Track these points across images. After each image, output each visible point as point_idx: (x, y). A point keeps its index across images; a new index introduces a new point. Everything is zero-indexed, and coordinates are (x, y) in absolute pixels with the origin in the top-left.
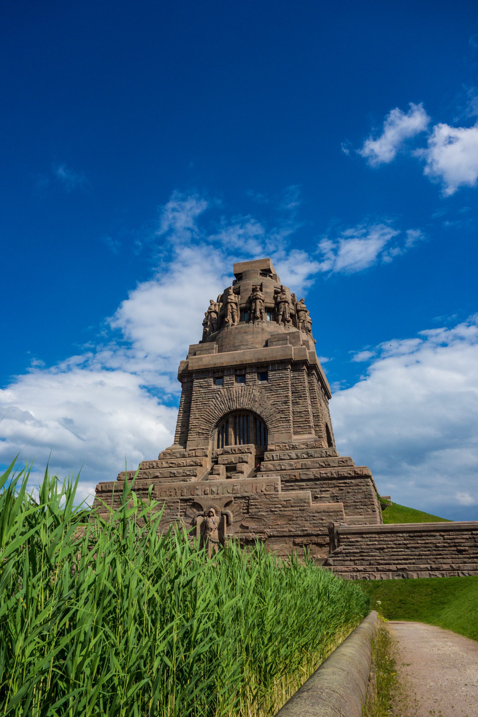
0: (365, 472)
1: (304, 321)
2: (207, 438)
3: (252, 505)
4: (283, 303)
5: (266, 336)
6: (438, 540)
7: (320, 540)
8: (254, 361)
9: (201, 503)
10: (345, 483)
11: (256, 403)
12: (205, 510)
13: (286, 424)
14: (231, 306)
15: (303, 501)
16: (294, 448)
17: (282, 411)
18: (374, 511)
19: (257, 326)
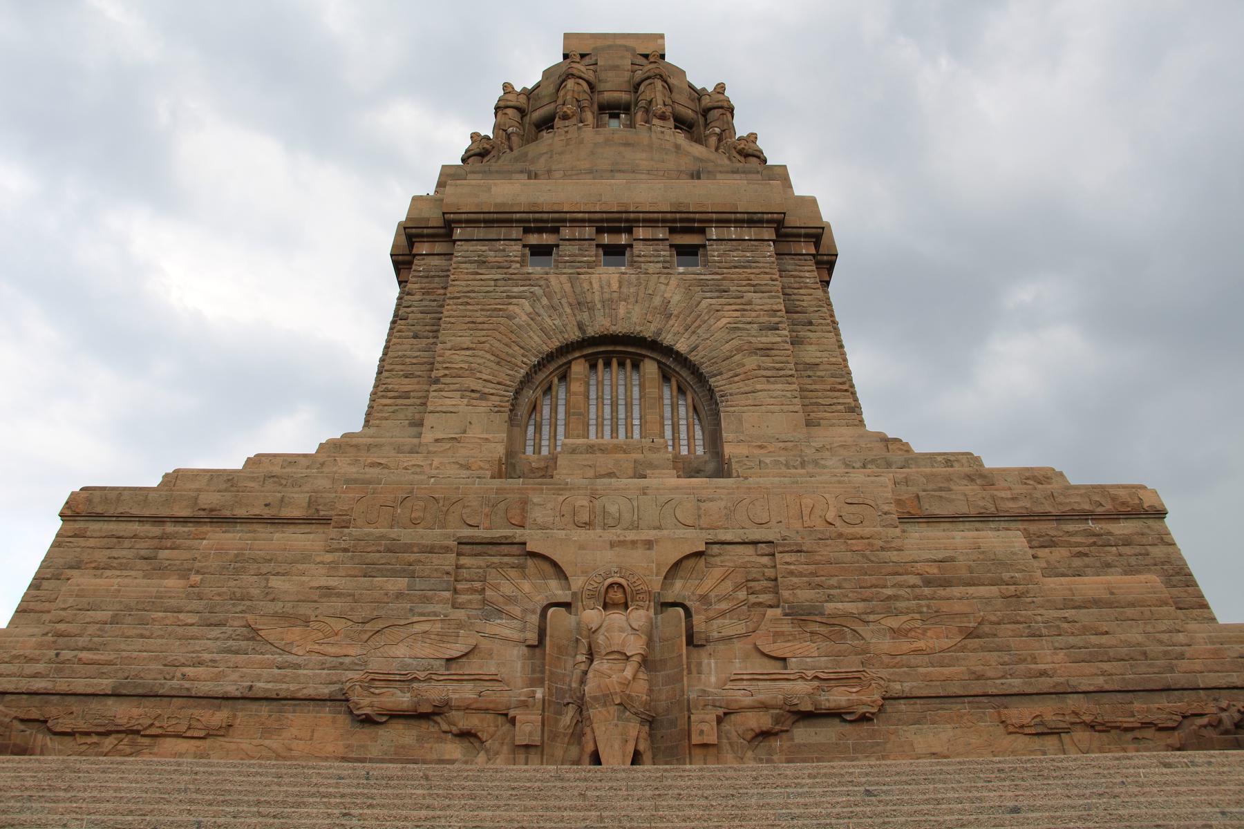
11: (671, 322)
12: (577, 583)
13: (779, 386)
17: (766, 350)
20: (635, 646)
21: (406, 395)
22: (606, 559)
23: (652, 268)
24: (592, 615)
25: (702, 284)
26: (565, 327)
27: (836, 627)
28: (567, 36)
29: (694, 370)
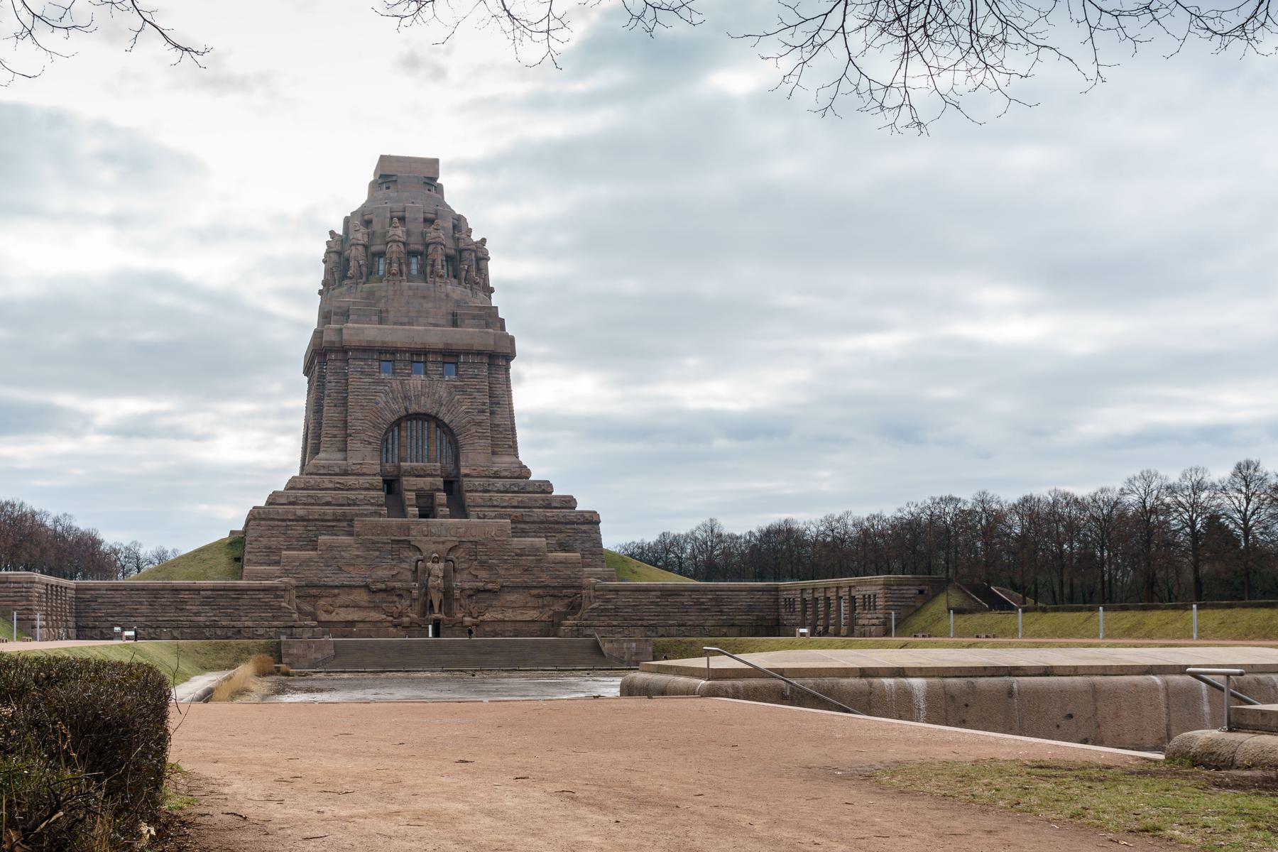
5: (450, 307)
6: (686, 600)
7: (555, 592)
8: (441, 346)
9: (420, 546)
15: (535, 550)
16: (497, 476)
17: (479, 424)
20: (441, 575)
21: (335, 436)
22: (433, 547)
23: (436, 377)
24: (429, 564)
25: (455, 387)
26: (399, 408)
27: (491, 568)
28: (383, 158)
29: (451, 430)
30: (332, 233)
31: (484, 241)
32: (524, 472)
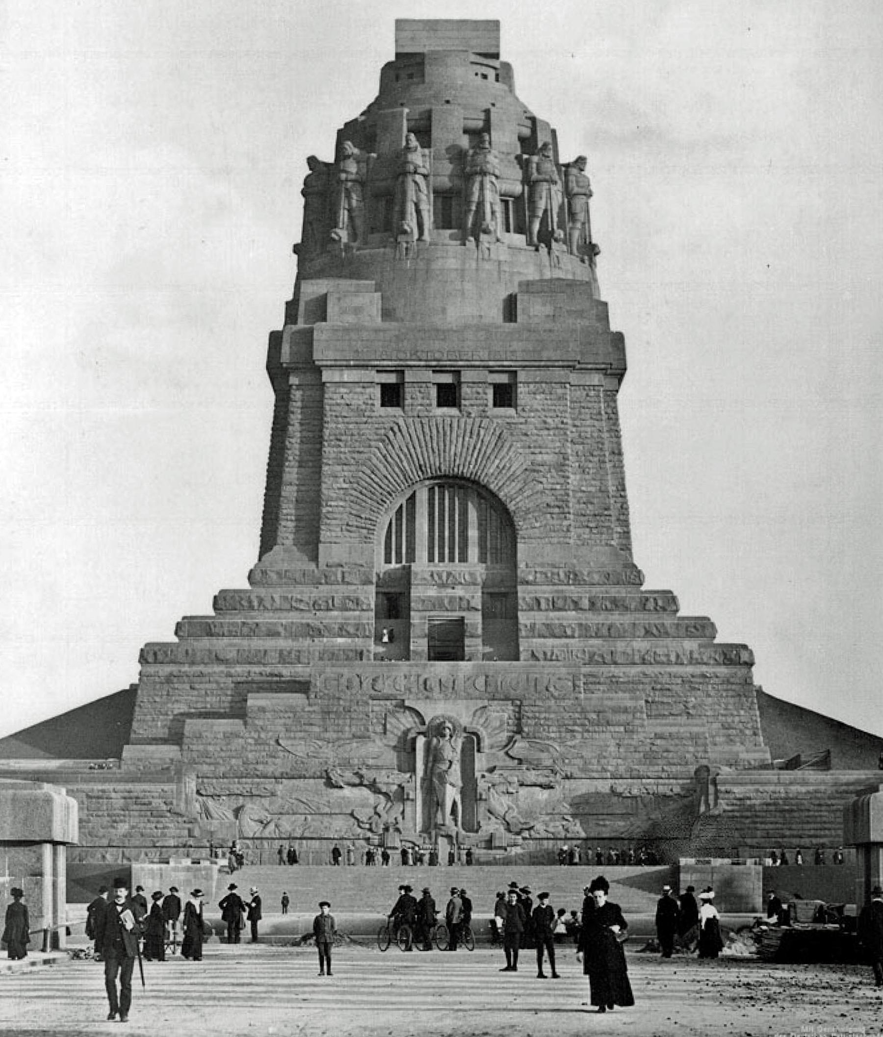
0: (745, 657)
1: (583, 224)
2: (367, 539)
3: (528, 718)
4: (545, 186)
10: (704, 676)
14: (416, 183)
18: (755, 734)
19: (486, 256)
28: (400, 24)
30: (312, 161)
31: (581, 162)
32: (636, 576)
